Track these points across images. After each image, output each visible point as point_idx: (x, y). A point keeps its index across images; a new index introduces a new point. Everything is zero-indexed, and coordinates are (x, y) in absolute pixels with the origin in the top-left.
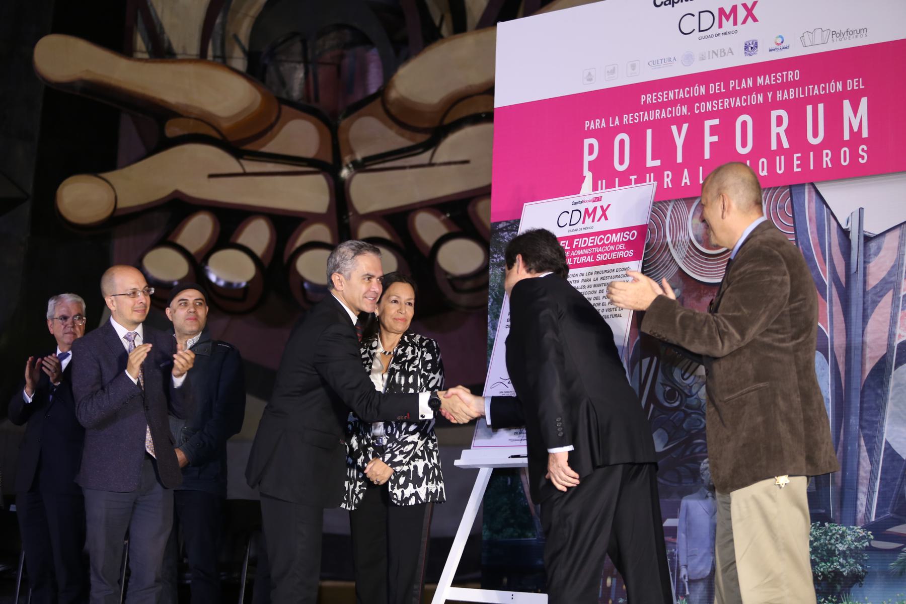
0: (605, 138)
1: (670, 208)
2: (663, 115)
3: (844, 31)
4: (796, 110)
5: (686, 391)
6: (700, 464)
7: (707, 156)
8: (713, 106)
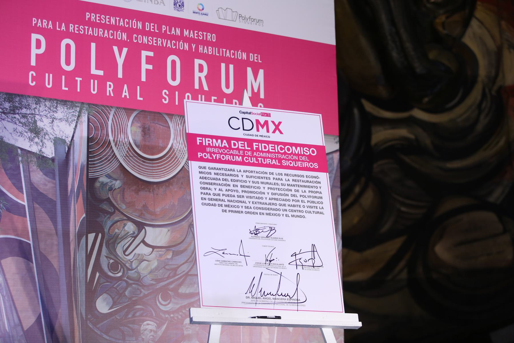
0: (53, 39)
1: (112, 113)
2: (106, 35)
3: (247, 17)
4: (214, 64)
5: (127, 265)
6: (140, 326)
7: (143, 79)
8: (148, 41)
